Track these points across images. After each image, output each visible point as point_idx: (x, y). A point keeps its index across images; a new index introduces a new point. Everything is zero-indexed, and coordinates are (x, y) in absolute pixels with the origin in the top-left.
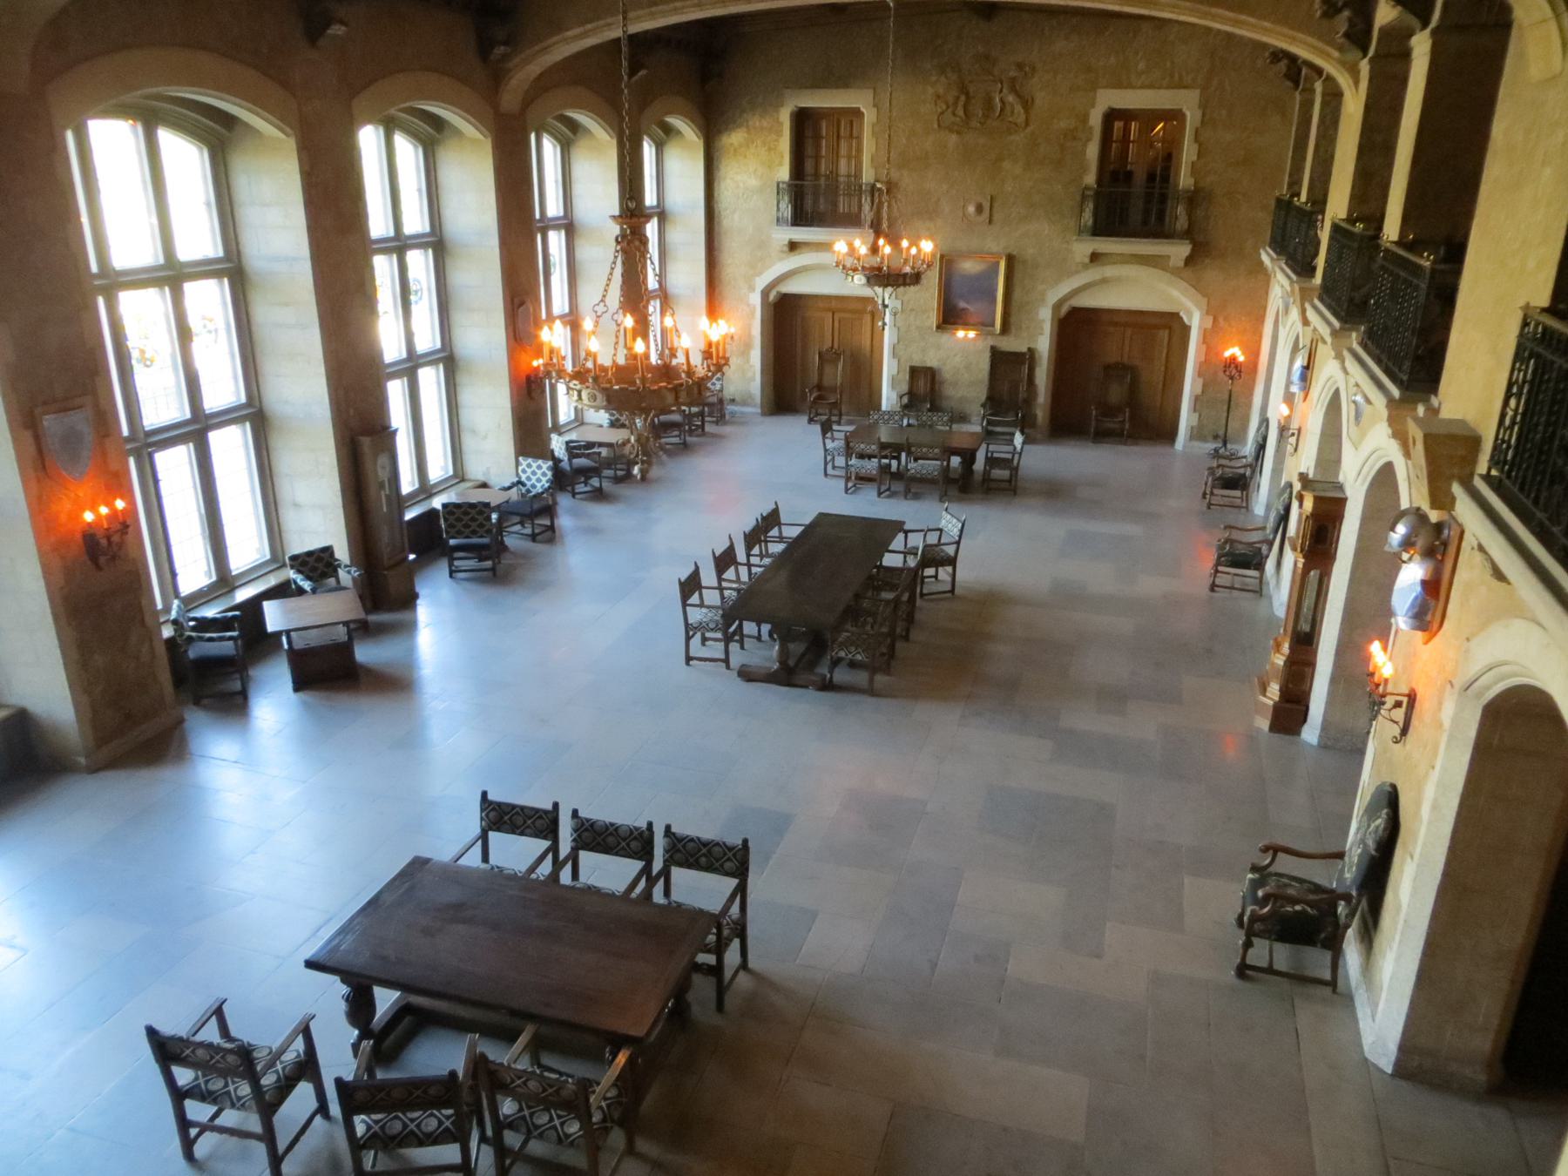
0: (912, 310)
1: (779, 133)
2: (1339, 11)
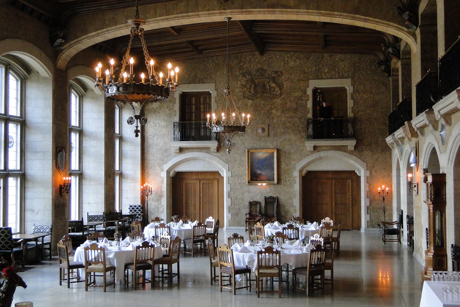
0: (236, 175)
1: (174, 102)
2: (404, 12)
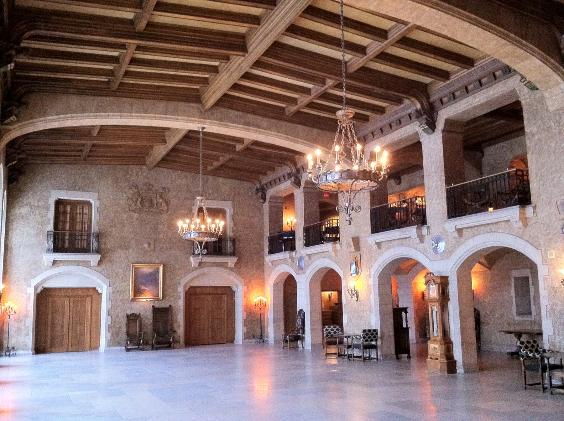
0: (118, 291)
